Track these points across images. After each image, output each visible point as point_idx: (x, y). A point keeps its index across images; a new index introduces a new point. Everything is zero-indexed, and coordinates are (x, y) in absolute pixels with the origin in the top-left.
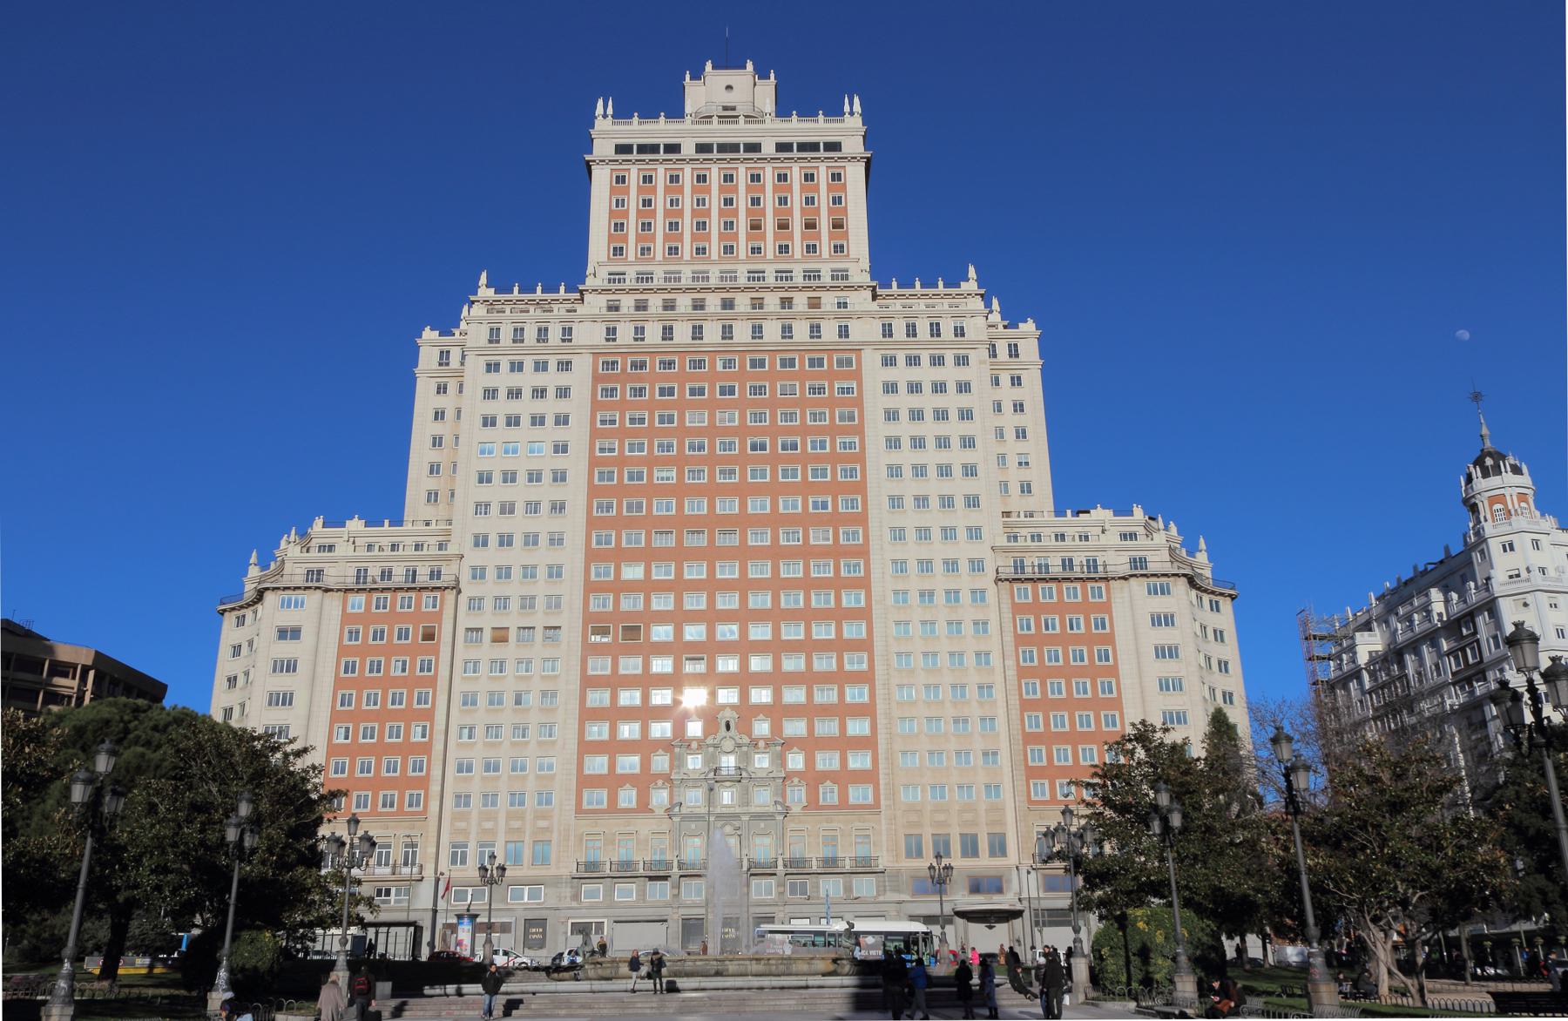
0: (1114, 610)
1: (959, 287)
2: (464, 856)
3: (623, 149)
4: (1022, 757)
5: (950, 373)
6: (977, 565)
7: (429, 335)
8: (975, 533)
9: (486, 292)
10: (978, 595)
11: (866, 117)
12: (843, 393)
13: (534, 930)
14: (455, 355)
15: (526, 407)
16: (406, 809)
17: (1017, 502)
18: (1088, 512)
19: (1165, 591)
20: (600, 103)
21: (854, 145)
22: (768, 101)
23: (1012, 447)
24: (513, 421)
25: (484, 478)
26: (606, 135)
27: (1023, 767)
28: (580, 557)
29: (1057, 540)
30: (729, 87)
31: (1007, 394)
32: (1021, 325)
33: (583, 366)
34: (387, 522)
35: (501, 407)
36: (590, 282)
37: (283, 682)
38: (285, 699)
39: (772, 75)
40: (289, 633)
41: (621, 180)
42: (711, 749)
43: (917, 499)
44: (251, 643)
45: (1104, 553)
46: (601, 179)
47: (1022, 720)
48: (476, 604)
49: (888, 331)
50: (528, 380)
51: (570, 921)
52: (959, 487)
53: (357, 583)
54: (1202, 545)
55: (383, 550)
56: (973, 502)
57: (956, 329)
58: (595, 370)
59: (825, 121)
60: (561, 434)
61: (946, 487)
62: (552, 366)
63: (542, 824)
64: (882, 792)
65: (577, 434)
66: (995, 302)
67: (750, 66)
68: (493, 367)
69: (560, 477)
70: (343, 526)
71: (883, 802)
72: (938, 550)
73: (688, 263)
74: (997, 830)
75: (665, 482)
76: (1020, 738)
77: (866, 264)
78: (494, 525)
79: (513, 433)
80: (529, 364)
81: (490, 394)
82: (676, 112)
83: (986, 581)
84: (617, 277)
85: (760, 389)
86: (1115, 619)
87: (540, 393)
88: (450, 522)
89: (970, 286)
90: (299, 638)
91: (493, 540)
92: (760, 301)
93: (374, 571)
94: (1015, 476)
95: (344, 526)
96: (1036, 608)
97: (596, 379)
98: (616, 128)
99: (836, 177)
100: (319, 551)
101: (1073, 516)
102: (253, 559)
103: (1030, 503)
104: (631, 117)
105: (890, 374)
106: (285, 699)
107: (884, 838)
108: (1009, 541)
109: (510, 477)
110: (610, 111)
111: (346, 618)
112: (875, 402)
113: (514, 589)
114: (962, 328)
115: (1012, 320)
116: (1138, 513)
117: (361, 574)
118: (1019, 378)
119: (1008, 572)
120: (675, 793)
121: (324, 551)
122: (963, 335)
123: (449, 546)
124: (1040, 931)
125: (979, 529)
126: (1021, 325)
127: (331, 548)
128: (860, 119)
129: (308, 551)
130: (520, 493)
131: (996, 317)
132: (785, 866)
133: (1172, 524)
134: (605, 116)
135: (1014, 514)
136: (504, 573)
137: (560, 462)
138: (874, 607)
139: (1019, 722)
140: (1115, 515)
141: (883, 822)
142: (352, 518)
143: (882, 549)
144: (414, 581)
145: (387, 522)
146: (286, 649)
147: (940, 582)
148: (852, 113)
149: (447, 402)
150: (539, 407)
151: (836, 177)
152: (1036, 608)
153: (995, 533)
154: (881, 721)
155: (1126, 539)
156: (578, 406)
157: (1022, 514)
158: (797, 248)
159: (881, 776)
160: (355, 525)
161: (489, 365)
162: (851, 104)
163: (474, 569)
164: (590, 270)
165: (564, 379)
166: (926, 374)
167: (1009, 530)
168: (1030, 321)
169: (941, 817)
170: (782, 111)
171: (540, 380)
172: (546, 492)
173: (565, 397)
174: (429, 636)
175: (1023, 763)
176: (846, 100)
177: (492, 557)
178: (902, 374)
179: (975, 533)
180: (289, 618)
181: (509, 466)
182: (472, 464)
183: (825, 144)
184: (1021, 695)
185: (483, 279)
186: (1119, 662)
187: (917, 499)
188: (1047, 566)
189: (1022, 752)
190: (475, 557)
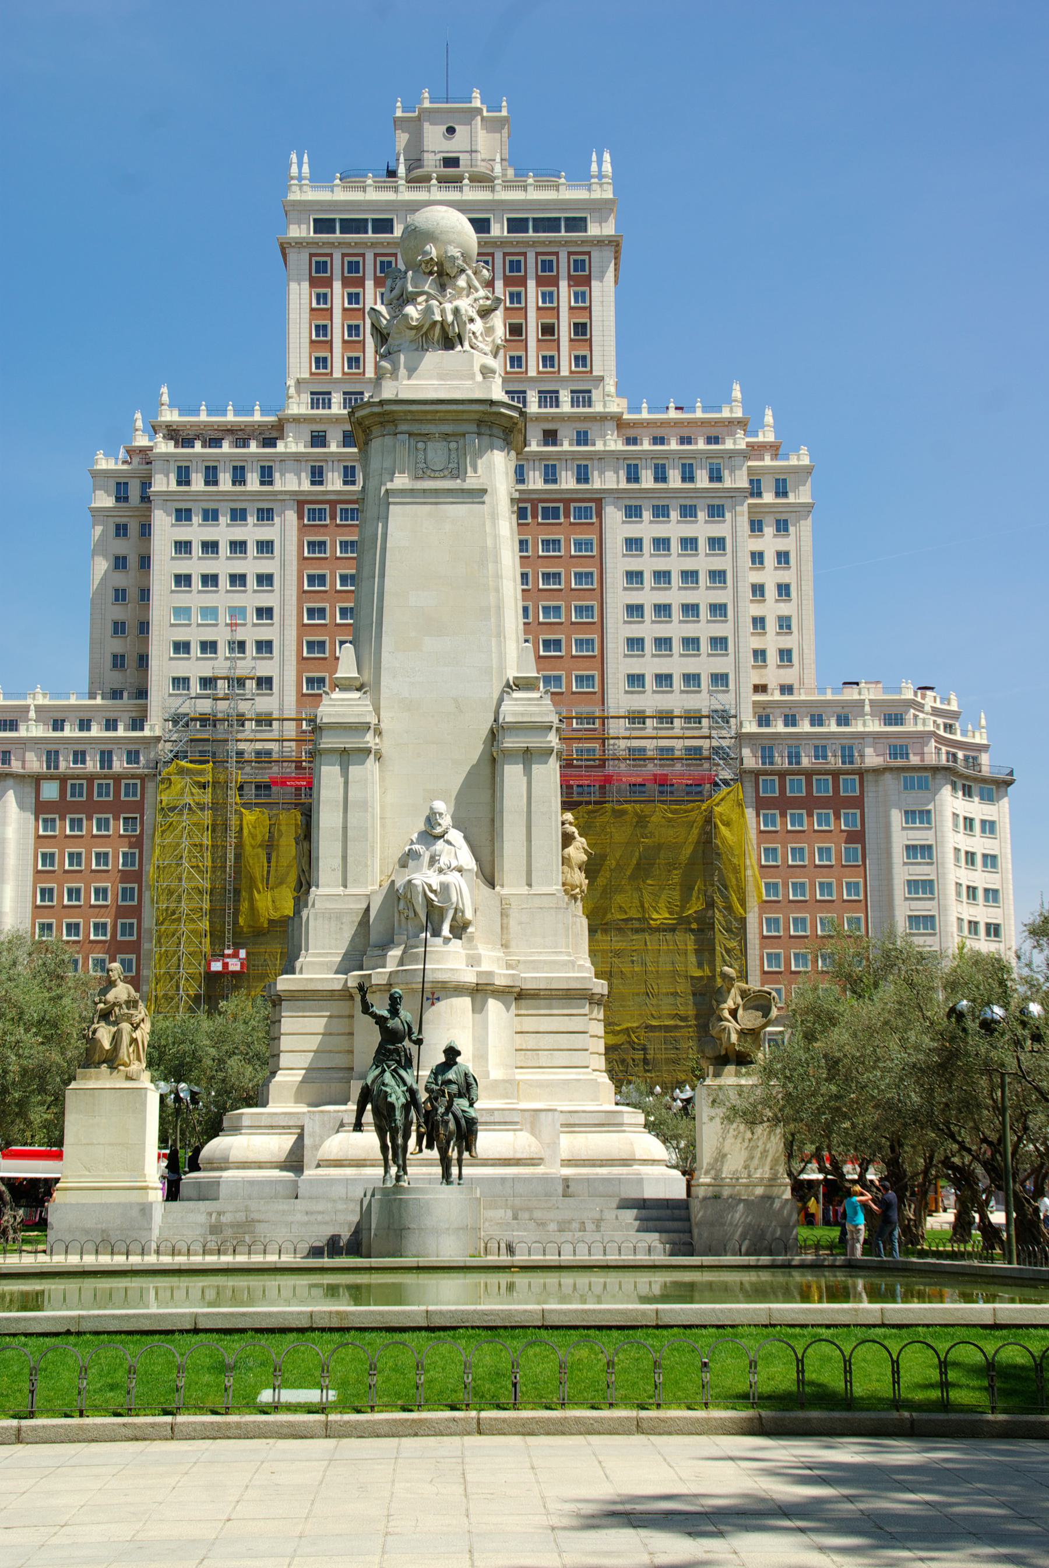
1: (721, 412)
3: (323, 225)
5: (702, 528)
17: (773, 675)
19: (924, 786)
20: (294, 157)
24: (210, 580)
27: (758, 973)
30: (451, 130)
35: (196, 566)
39: (504, 104)
45: (861, 741)
49: (633, 476)
54: (983, 722)
76: (757, 942)
79: (210, 599)
94: (772, 642)
97: (303, 529)
99: (579, 265)
103: (788, 676)
105: (634, 530)
110: (306, 169)
123: (147, 728)
128: (610, 188)
139: (756, 925)
151: (579, 265)
157: (777, 692)
161: (178, 511)
165: (266, 533)
166: (674, 528)
168: (804, 450)
171: (238, 533)
176: (594, 157)
178: (647, 529)
181: (209, 635)
183: (567, 219)
189: (758, 958)
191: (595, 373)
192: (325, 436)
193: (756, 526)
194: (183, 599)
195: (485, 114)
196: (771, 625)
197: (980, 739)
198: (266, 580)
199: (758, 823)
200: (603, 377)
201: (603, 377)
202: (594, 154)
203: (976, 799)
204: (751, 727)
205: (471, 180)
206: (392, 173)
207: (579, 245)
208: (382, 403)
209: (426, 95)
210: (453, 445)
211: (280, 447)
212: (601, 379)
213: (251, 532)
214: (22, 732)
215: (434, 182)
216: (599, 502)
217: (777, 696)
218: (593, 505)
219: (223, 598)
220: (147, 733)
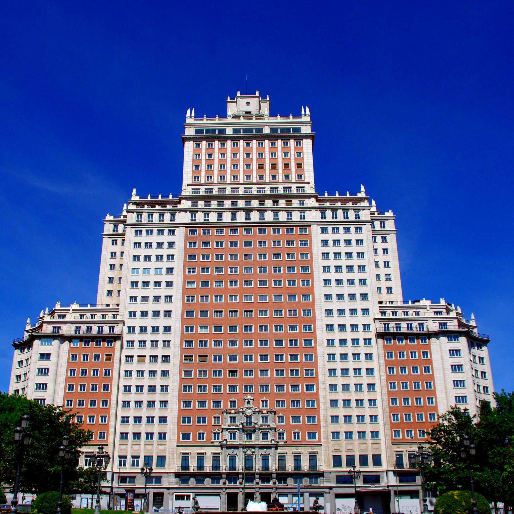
0: (432, 348)
1: (357, 195)
2: (125, 461)
4: (389, 419)
5: (353, 236)
6: (366, 327)
7: (109, 217)
8: (365, 312)
9: (135, 198)
10: (367, 341)
11: (311, 116)
13: (158, 498)
14: (121, 227)
15: (154, 251)
16: (98, 439)
17: (385, 297)
18: (419, 301)
20: (189, 111)
21: (306, 130)
22: (266, 109)
23: (383, 271)
24: (148, 258)
25: (134, 284)
26: (191, 125)
27: (389, 423)
28: (179, 322)
29: (404, 315)
30: (248, 103)
31: (380, 245)
33: (181, 232)
34: (89, 305)
35: (143, 252)
36: (183, 193)
37: (42, 379)
38: (42, 386)
40: (45, 356)
41: (198, 145)
42: (241, 414)
43: (338, 295)
44: (27, 360)
46: (189, 146)
47: (389, 401)
48: (130, 343)
49: (323, 216)
50: (155, 238)
51: (175, 494)
52: (357, 290)
53: (76, 333)
54: (473, 317)
55: (87, 318)
56: (364, 296)
57: (356, 215)
58: (186, 234)
59: (293, 118)
60: (170, 265)
61: (352, 290)
63: (161, 448)
64: (322, 435)
65: (178, 264)
66: (374, 203)
67: (257, 94)
68: (138, 233)
69: (169, 284)
70: (70, 307)
71: (322, 440)
72: (348, 320)
74: (377, 453)
75: (219, 287)
76: (388, 409)
77: (312, 184)
78: (139, 307)
79: (147, 265)
80: (155, 231)
81: (137, 245)
82: (224, 115)
83: (371, 335)
86: (432, 353)
87: (160, 244)
88: (118, 305)
89: (362, 195)
90: (50, 359)
91: (138, 314)
93: (84, 328)
94: (384, 284)
95: (70, 307)
96: (394, 347)
97: (186, 238)
100: (58, 318)
101: (412, 303)
102: (28, 321)
103: (391, 297)
104: (203, 117)
105: (325, 237)
106: (42, 386)
107: (323, 457)
108: (382, 315)
109: (146, 284)
110: (193, 114)
111: (70, 349)
112: (318, 250)
113: (148, 337)
114: (358, 215)
115: (381, 209)
116: (443, 302)
117: (78, 328)
118: (385, 237)
119: (382, 330)
120: (224, 435)
121: (61, 318)
122: (359, 218)
123: (118, 316)
124: (398, 501)
125: (367, 310)
127: (64, 316)
129: (53, 317)
130: (151, 292)
131: (373, 209)
132: (276, 470)
133: (458, 307)
134: (191, 117)
135: (384, 303)
136: (143, 329)
137: (169, 278)
138: (318, 347)
139: (387, 402)
140: (432, 303)
141: (323, 449)
142: (73, 303)
143: (321, 319)
144: (102, 333)
145: (89, 305)
146: (44, 364)
147: (349, 335)
148: (305, 115)
149: (117, 249)
150: (160, 252)
152: (394, 347)
153: (375, 312)
154: (321, 401)
155: (437, 315)
156: (179, 251)
157: (388, 303)
159: (322, 428)
160: (75, 306)
161: (136, 231)
162: (305, 111)
163: (129, 327)
164: (183, 189)
166: (342, 236)
167: (382, 311)
168: (390, 211)
169: (350, 447)
170: (273, 114)
172: (163, 292)
174: (109, 357)
175: (389, 421)
176: (303, 109)
177: (138, 322)
178: (330, 236)
179: (365, 312)
180: (45, 349)
181: (146, 279)
182: (128, 277)
184: (388, 389)
185: (134, 192)
186: (435, 373)
187: (338, 295)
188: (400, 327)
190: (130, 323)
193: (374, 239)
194: (136, 265)
195: (261, 100)
196: (383, 277)
197: (473, 323)
198: (171, 257)
199: (385, 357)
200: (309, 182)
201: (309, 182)
203: (476, 348)
204: (379, 316)
205: (256, 116)
207: (298, 137)
211: (179, 207)
212: (309, 183)
213: (166, 238)
214: (67, 319)
216: (310, 226)
217: (388, 305)
219: (153, 264)
220: (119, 318)
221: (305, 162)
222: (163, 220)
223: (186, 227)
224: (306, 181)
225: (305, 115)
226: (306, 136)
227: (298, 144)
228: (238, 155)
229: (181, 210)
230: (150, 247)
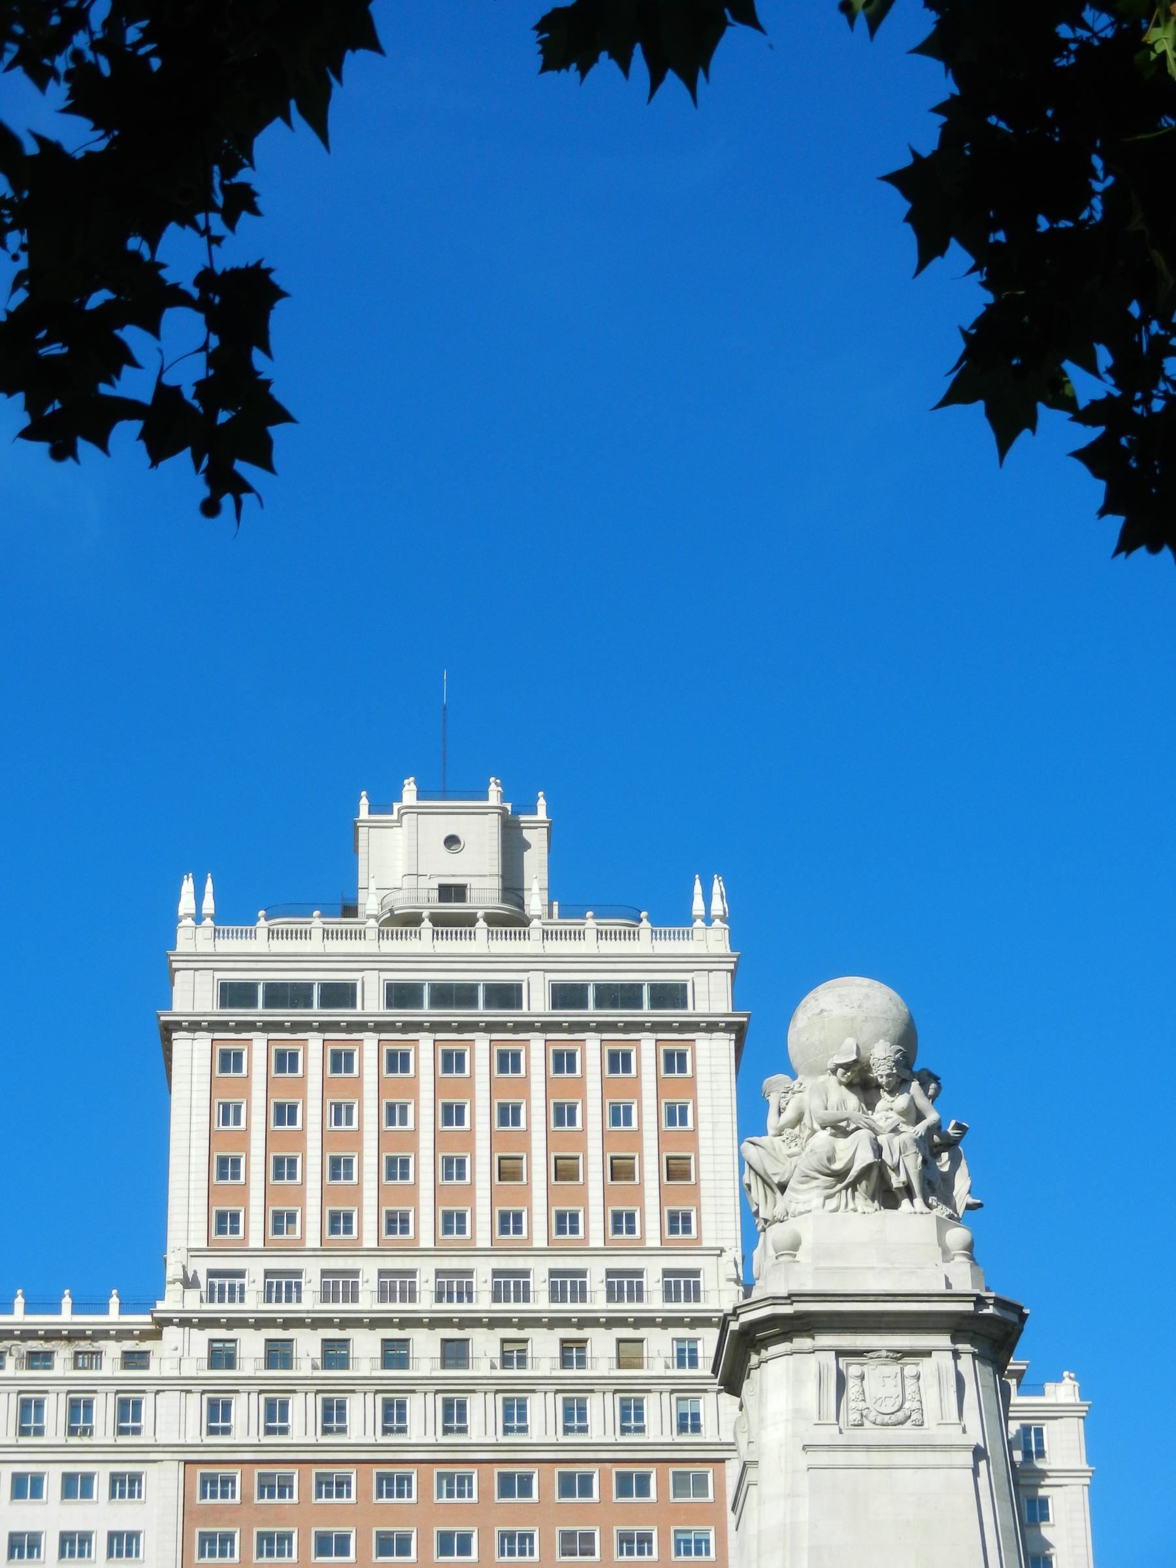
12: (688, 1552)
20: (188, 887)
30: (452, 841)
32: (1049, 1387)
36: (173, 1301)
39: (542, 804)
41: (230, 1061)
62: (101, 1486)
73: (371, 1253)
84: (227, 1282)
85: (522, 1541)
92: (521, 1346)
98: (226, 945)
104: (253, 921)
110: (209, 905)
126: (1049, 1387)
158: (595, 1226)
173: (129, 1554)
176: (698, 888)
183: (656, 989)
191: (705, 1244)
192: (234, 1349)
202: (698, 882)
206: (350, 910)
208: (791, 1298)
209: (413, 787)
210: (910, 1370)
215: (427, 924)
218: (709, 1470)
221: (702, 1151)
222: (87, 1431)
223: (186, 1462)
224: (705, 1244)
225: (708, 920)
226: (711, 1028)
227: (674, 1061)
228: (411, 1110)
229: (162, 1386)
230: (30, 1555)
